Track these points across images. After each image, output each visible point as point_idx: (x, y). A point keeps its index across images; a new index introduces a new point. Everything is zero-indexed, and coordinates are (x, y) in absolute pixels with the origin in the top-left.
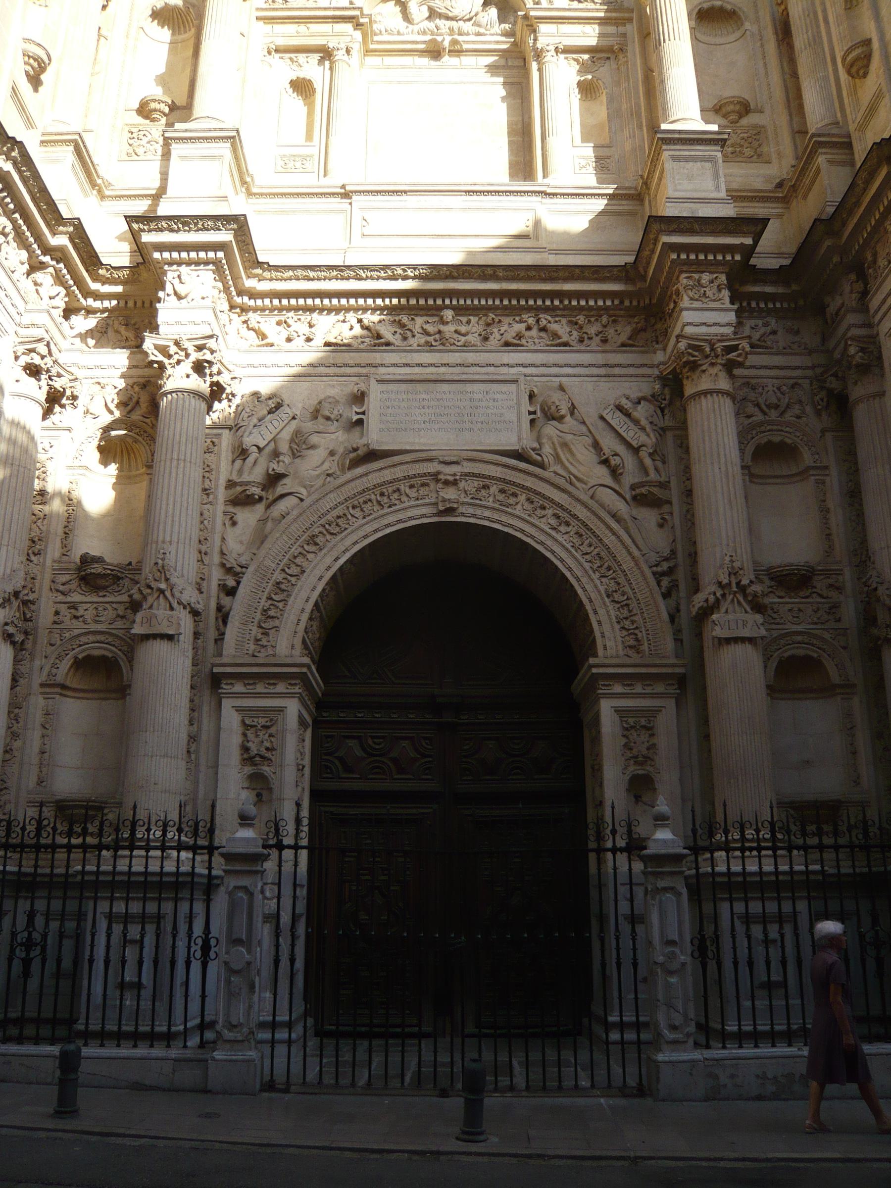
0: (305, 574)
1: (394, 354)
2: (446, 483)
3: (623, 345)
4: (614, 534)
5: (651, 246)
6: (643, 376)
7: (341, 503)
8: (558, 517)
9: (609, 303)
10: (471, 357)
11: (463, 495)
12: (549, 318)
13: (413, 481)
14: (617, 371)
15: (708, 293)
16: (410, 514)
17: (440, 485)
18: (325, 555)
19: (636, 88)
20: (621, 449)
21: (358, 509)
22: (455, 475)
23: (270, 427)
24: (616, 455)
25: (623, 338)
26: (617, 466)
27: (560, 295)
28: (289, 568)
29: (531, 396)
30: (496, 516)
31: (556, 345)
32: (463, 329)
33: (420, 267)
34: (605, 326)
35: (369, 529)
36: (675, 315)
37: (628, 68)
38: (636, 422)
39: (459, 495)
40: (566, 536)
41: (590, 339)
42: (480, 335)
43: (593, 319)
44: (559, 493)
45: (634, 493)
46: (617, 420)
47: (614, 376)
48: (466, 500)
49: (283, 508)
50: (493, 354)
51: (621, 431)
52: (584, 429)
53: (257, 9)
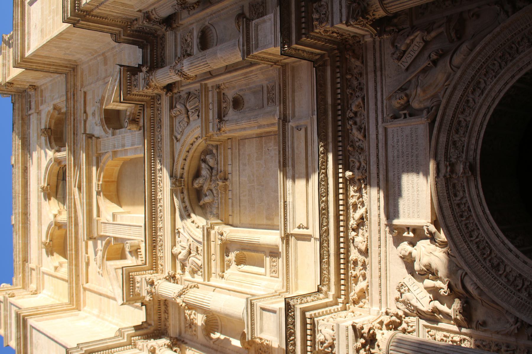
0: (522, 274)
1: (372, 208)
2: (452, 171)
3: (362, 63)
4: (484, 48)
5: (300, 52)
6: (380, 47)
7: (468, 246)
8: (474, 90)
9: (338, 75)
10: (373, 159)
11: (461, 159)
12: (349, 111)
13: (452, 195)
14: (378, 64)
15: (324, 12)
16: (475, 197)
17: (454, 176)
18: (507, 258)
19: (234, 77)
20: (426, 54)
21: (472, 233)
22: (447, 167)
23: (418, 291)
24: (429, 56)
25: (358, 63)
26: (437, 53)
27: (334, 106)
28: (517, 286)
29: (395, 117)
30: (475, 134)
31: (364, 105)
32: (357, 164)
33: (320, 193)
34: (352, 75)
35: (486, 226)
36: (340, 32)
37: (227, 83)
38: (408, 46)
39: (461, 162)
40: (488, 83)
41: (360, 84)
42: (360, 153)
43: (349, 84)
44: (456, 92)
45: (455, 40)
46: (407, 60)
47: (381, 65)
48: (464, 157)
49: (472, 287)
50: (371, 144)
51: (415, 55)
52: (414, 80)
53: (204, 280)
